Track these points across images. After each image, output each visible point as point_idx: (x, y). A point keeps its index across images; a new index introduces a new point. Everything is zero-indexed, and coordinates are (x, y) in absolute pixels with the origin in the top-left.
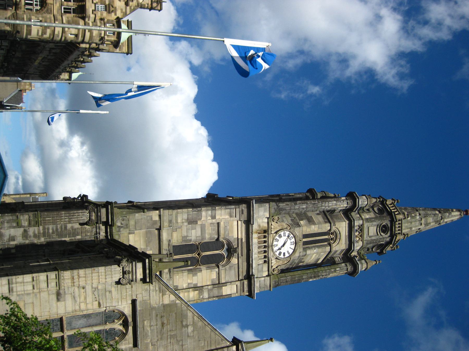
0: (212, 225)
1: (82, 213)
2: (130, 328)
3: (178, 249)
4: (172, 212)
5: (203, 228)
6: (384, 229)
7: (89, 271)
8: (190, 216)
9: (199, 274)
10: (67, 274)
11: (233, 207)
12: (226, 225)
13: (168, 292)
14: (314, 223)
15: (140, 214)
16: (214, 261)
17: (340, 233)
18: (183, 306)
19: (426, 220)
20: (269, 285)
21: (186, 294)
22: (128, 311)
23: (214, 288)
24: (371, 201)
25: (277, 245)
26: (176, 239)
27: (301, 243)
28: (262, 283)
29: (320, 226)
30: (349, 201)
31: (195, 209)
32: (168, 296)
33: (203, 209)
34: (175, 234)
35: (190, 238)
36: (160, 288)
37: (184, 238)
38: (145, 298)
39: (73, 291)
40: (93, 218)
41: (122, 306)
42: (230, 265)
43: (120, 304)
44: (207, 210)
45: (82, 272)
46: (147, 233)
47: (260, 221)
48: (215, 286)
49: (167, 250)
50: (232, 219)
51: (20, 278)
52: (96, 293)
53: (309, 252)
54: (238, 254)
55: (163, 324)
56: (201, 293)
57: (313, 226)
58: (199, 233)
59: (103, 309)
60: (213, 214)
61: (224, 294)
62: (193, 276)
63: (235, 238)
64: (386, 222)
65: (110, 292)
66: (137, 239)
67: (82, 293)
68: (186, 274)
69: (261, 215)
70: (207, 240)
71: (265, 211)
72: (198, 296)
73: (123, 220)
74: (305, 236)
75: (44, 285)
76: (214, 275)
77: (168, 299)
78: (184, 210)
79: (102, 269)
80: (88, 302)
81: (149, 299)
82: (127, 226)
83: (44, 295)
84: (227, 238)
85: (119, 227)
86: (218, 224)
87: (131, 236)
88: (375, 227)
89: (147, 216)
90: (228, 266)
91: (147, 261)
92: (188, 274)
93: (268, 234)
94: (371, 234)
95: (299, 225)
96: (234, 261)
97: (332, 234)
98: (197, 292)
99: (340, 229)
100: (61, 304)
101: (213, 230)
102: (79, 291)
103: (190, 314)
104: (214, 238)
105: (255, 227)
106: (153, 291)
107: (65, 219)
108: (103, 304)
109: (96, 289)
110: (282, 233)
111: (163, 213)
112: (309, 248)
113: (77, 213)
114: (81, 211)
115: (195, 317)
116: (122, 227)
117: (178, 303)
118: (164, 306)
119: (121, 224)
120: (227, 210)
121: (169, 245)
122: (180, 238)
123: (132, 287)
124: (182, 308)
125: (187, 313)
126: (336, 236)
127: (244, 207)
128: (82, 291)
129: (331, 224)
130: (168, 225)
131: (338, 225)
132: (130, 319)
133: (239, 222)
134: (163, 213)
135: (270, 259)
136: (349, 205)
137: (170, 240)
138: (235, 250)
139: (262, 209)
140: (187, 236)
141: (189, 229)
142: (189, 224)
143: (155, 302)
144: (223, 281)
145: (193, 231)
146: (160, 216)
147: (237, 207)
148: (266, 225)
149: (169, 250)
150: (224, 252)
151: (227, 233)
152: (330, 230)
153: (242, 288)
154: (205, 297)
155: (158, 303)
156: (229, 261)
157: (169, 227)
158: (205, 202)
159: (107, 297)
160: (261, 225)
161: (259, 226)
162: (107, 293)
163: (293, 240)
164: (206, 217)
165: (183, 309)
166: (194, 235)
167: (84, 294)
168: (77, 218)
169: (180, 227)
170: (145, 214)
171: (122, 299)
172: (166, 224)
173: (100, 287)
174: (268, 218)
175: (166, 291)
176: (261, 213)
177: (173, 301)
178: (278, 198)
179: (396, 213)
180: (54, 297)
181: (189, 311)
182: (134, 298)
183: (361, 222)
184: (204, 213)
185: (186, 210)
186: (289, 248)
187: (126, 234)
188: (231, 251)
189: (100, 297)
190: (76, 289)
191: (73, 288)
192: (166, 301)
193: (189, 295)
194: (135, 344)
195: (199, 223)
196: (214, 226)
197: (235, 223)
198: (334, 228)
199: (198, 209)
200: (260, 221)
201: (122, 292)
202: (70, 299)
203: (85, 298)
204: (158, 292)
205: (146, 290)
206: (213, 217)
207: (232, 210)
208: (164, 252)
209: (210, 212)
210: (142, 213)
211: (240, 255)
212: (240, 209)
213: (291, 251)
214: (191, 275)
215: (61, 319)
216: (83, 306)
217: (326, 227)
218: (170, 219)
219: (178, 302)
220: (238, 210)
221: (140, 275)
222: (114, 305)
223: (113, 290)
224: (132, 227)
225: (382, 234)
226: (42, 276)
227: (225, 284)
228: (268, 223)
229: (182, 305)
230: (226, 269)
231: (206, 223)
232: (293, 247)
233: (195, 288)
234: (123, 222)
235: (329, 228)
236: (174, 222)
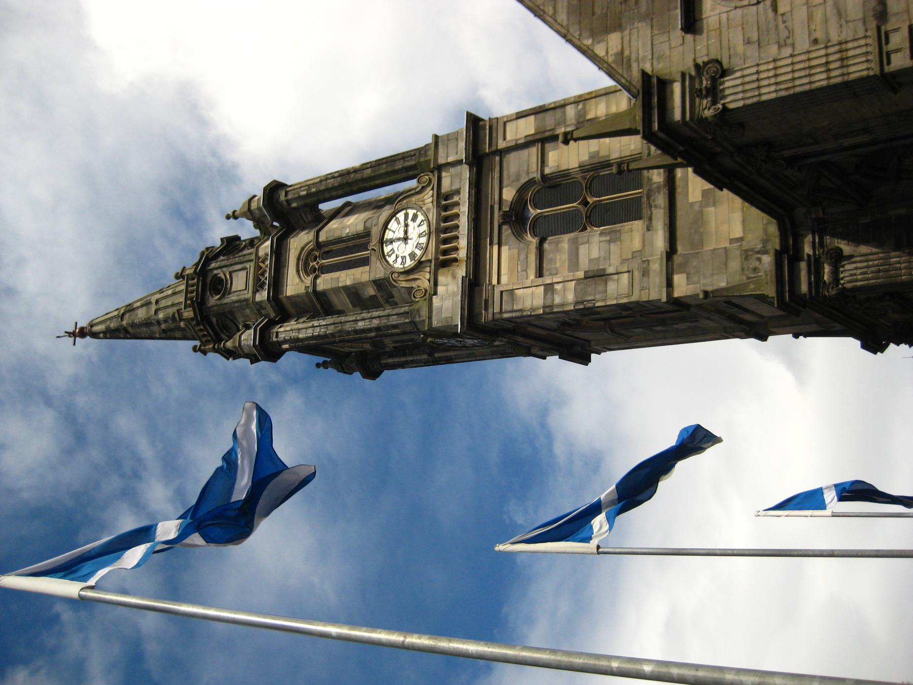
0: (554, 272)
1: (856, 281)
3: (632, 211)
4: (640, 296)
7: (802, 85)
8: (601, 288)
10: (859, 69)
11: (505, 316)
12: (524, 273)
13: (610, 60)
14: (346, 288)
15: (715, 288)
17: (298, 271)
18: (577, 35)
19: (148, 312)
20: (440, 147)
21: (614, 109)
23: (553, 130)
24: (234, 342)
25: (420, 236)
26: (633, 233)
28: (452, 151)
29: (334, 285)
30: (275, 339)
31: (590, 305)
32: (611, 52)
33: (572, 308)
34: (637, 244)
35: (603, 238)
36: (629, 66)
37: (615, 238)
38: (664, 38)
39: (844, 29)
40: (827, 269)
41: (717, 11)
42: (519, 185)
43: (724, 16)
44: (563, 305)
45: (820, 80)
46: (701, 243)
48: (551, 133)
49: (656, 206)
50: (510, 288)
52: (784, 34)
53: (360, 228)
54: (500, 209)
56: (580, 116)
57: (348, 283)
58: (583, 250)
60: (549, 296)
61: (532, 118)
62: (598, 152)
63: (506, 245)
64: (213, 300)
65: (748, 42)
66: (724, 228)
67: (818, 28)
69: (447, 300)
70: (566, 237)
71: (440, 309)
72: (588, 107)
73: (755, 269)
74: (365, 262)
77: (610, 44)
78: (614, 302)
79: (769, 93)
80: (805, 8)
81: (655, 37)
82: (746, 255)
84: (522, 245)
85: (765, 252)
86: (540, 273)
87: (738, 232)
88: (234, 289)
89: (698, 282)
90: (524, 180)
91: (656, 126)
92: (609, 156)
93: (436, 259)
94: (243, 273)
95: (379, 284)
96: (509, 194)
97: (314, 270)
98: (590, 116)
99: (297, 280)
101: (551, 260)
102: (827, 33)
104: (549, 244)
106: (644, 58)
107: (899, 262)
108: (765, 10)
109: (782, 42)
110: (409, 263)
111: (660, 292)
112: (358, 236)
113: (868, 279)
114: (859, 284)
115: (550, 10)
116: (758, 252)
117: (588, 38)
118: (619, 27)
119: (759, 260)
120: (520, 307)
121: (650, 219)
122: (625, 236)
123: (695, 60)
124: (580, 29)
125: (568, 19)
126: (306, 265)
127: (486, 317)
128: (819, 35)
129: (314, 291)
130: (651, 263)
133: (495, 281)
134: (661, 294)
135: (435, 203)
136: (275, 330)
137: (648, 229)
138: (506, 218)
139: (445, 314)
140: (609, 242)
141: (605, 258)
142: (604, 270)
143: (641, 33)
145: (595, 254)
146: (670, 284)
147: (497, 316)
148: (441, 279)
149: (651, 206)
150: (533, 212)
151: (522, 257)
152: (316, 278)
153: (494, 135)
154: (573, 106)
155: (634, 32)
156: (522, 190)
157: (648, 261)
158: (589, 341)
159: (755, 28)
160: (450, 278)
161: (454, 277)
162: (755, 37)
164: (564, 289)
165: (577, 27)
166: (593, 246)
167: (813, 27)
168: (867, 267)
169: (624, 261)
170: (702, 288)
171: (719, 28)
173: (773, 50)
174: (435, 293)
175: (614, 62)
176: (448, 304)
177: (599, 42)
178: (437, 355)
179: (194, 322)
181: (565, 23)
182: (689, 37)
184: (570, 297)
185: (609, 303)
186: (395, 229)
187: (750, 237)
189: (772, 24)
190: (835, 38)
191: (843, 38)
192: (614, 40)
193: (608, 106)
195: (580, 274)
196: (548, 270)
197: (504, 279)
198: (308, 281)
199: (581, 307)
201: (718, 44)
202: (850, 7)
203: (810, 18)
204: (633, 57)
205: (659, 58)
206: (549, 288)
207: (509, 309)
208: (661, 200)
209: (557, 300)
210: (709, 289)
211: (496, 207)
212: (490, 310)
214: (602, 154)
218: (645, 279)
219: (589, 42)
220: (497, 310)
222: (739, 11)
223: (740, 48)
225: (223, 277)
227: (529, 139)
228: (436, 284)
229: (580, 35)
230: (528, 173)
231: (566, 273)
234: (757, 264)
235: (318, 281)
236: (636, 274)
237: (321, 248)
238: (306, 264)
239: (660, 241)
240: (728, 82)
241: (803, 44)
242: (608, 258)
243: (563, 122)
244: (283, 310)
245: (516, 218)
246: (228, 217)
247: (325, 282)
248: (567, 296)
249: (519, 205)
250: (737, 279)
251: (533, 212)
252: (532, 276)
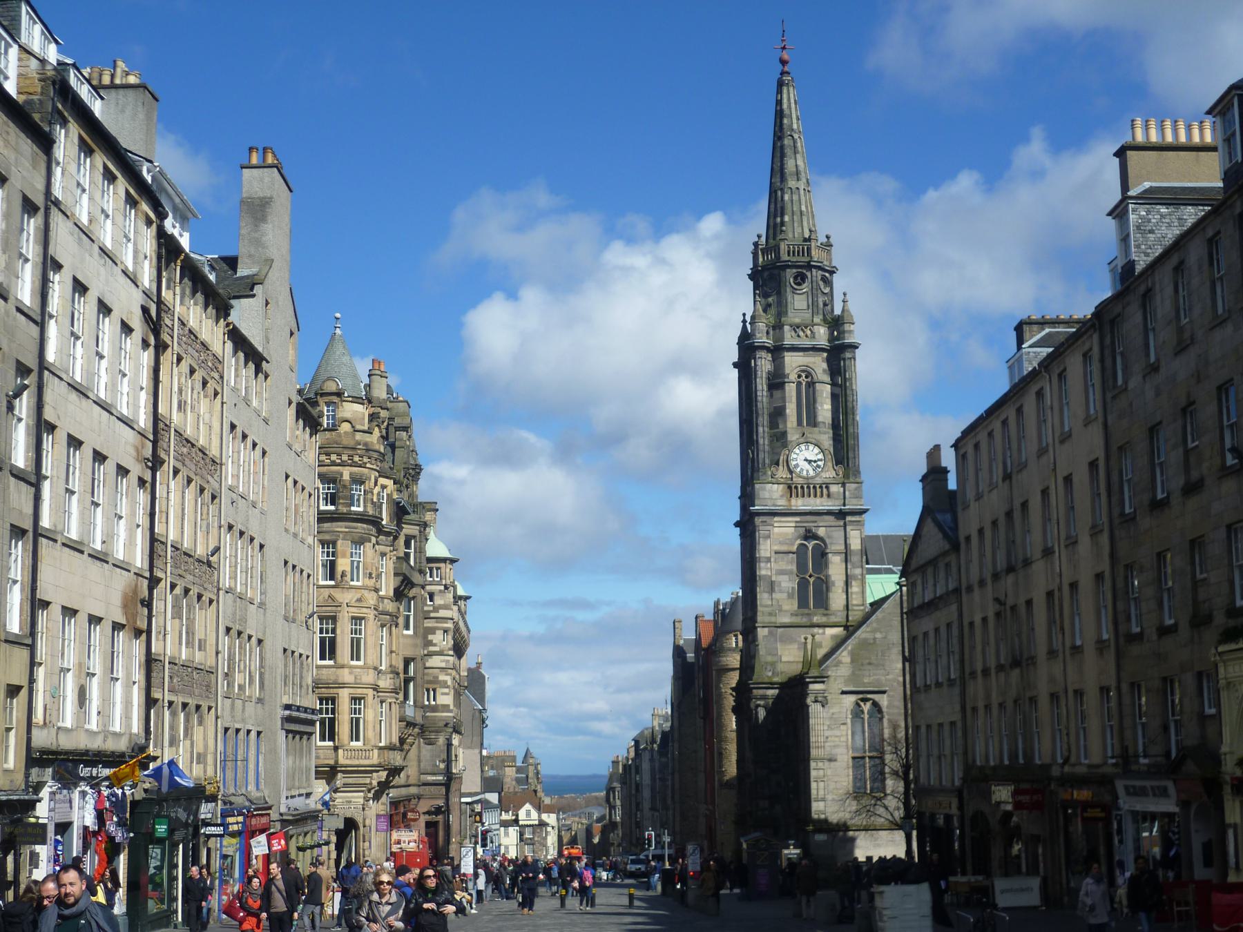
2: (869, 696)
3: (803, 603)
5: (781, 572)
7: (812, 733)
9: (833, 578)
10: (813, 752)
16: (821, 556)
22: (853, 698)
26: (792, 605)
27: (807, 430)
37: (790, 596)
40: (762, 703)
45: (813, 739)
46: (781, 641)
47: (776, 495)
51: (814, 792)
53: (820, 419)
55: (870, 664)
58: (786, 578)
59: (849, 721)
68: (831, 595)
70: (794, 567)
71: (764, 489)
74: (800, 423)
75: (821, 772)
79: (812, 721)
82: (773, 664)
83: (829, 772)
87: (784, 659)
90: (828, 541)
95: (784, 434)
96: (821, 532)
100: (839, 758)
103: (864, 636)
105: (781, 504)
112: (815, 417)
118: (852, 661)
131: (787, 371)
132: (861, 696)
138: (808, 531)
144: (843, 547)
145: (783, 584)
150: (811, 545)
156: (822, 539)
163: (803, 447)
166: (788, 583)
172: (773, 619)
176: (767, 495)
180: (833, 764)
183: (786, 328)
184: (763, 572)
186: (813, 453)
188: (809, 535)
192: (848, 660)
194: (884, 692)
197: (776, 530)
198: (793, 377)
200: (776, 495)
206: (768, 560)
208: (804, 620)
209: (762, 565)
213: (817, 450)
215: (854, 758)
216: (843, 739)
224: (775, 659)
226: (813, 773)
232: (811, 447)
237: (811, 385)
238: (803, 371)
239: (786, 620)
240: (819, 706)
241: (827, 733)
242: (781, 592)
243: (854, 567)
244: (777, 351)
245: (809, 535)
246: (845, 294)
247: (791, 389)
248: (763, 570)
249: (816, 537)
250: (763, 659)
252: (776, 548)
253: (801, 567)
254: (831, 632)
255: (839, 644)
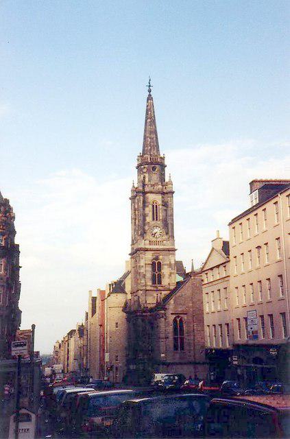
3: (154, 282)
6: (154, 169)
22: (174, 316)
26: (150, 283)
76: (166, 267)
96: (161, 257)
166: (149, 275)
172: (144, 288)
188: (157, 258)
194: (186, 314)
198: (151, 203)
208: (155, 289)
217: (151, 206)
221: (163, 312)
233: (170, 275)
239: (148, 288)
251: (157, 262)
253: (154, 270)
254: (163, 292)
255: (167, 298)
